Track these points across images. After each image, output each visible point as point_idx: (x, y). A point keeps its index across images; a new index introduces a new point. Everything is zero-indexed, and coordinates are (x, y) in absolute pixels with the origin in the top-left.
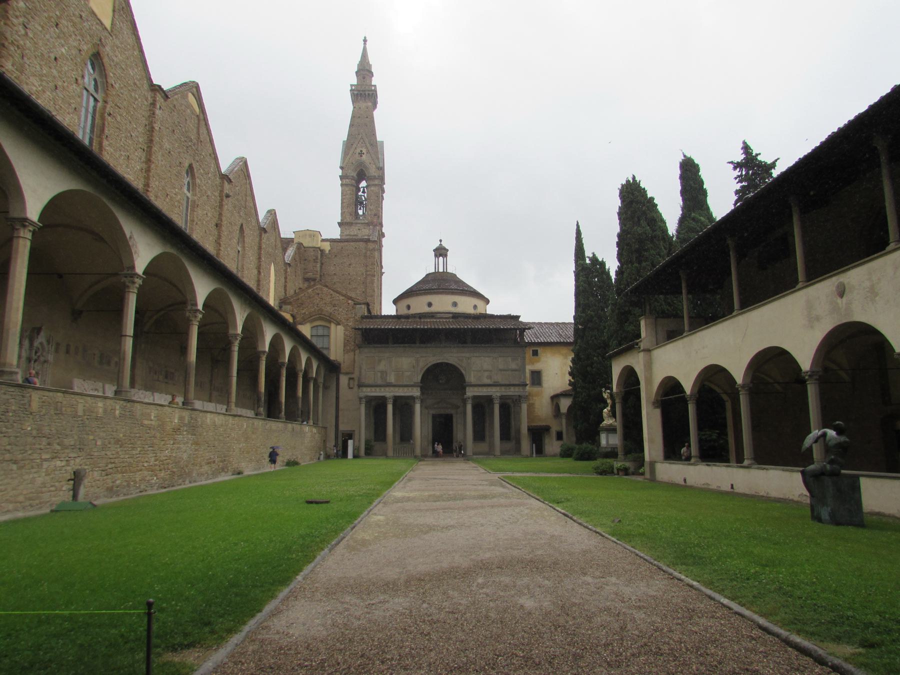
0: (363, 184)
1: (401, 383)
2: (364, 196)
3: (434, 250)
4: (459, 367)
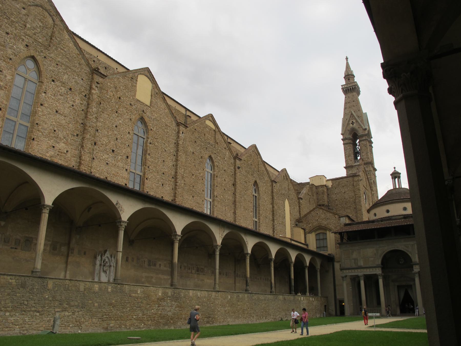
1: (368, 266)
2: (358, 148)
3: (391, 175)
4: (406, 251)
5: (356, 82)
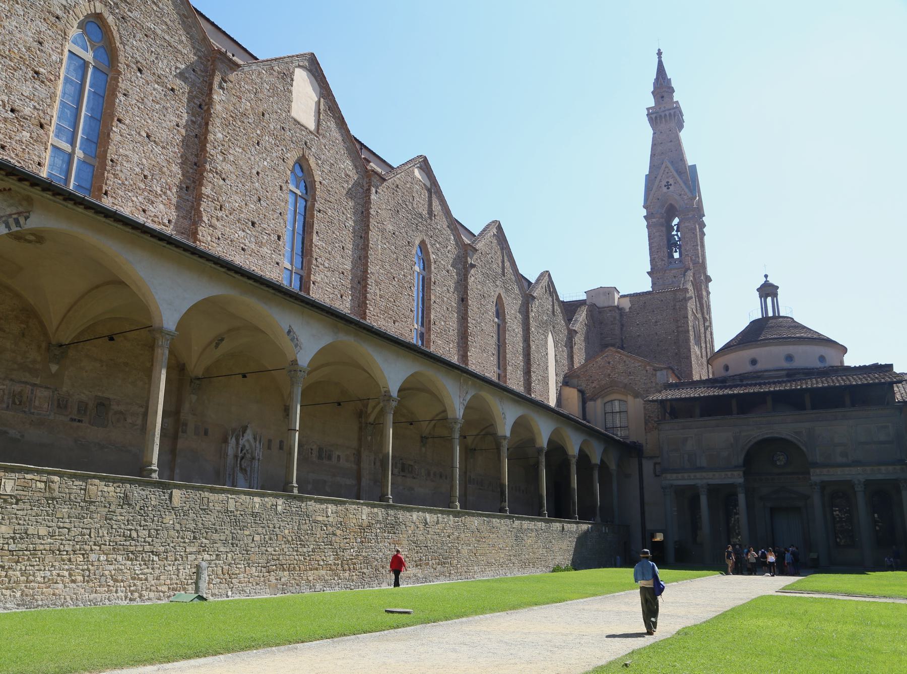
0: (676, 221)
2: (677, 235)
5: (677, 102)
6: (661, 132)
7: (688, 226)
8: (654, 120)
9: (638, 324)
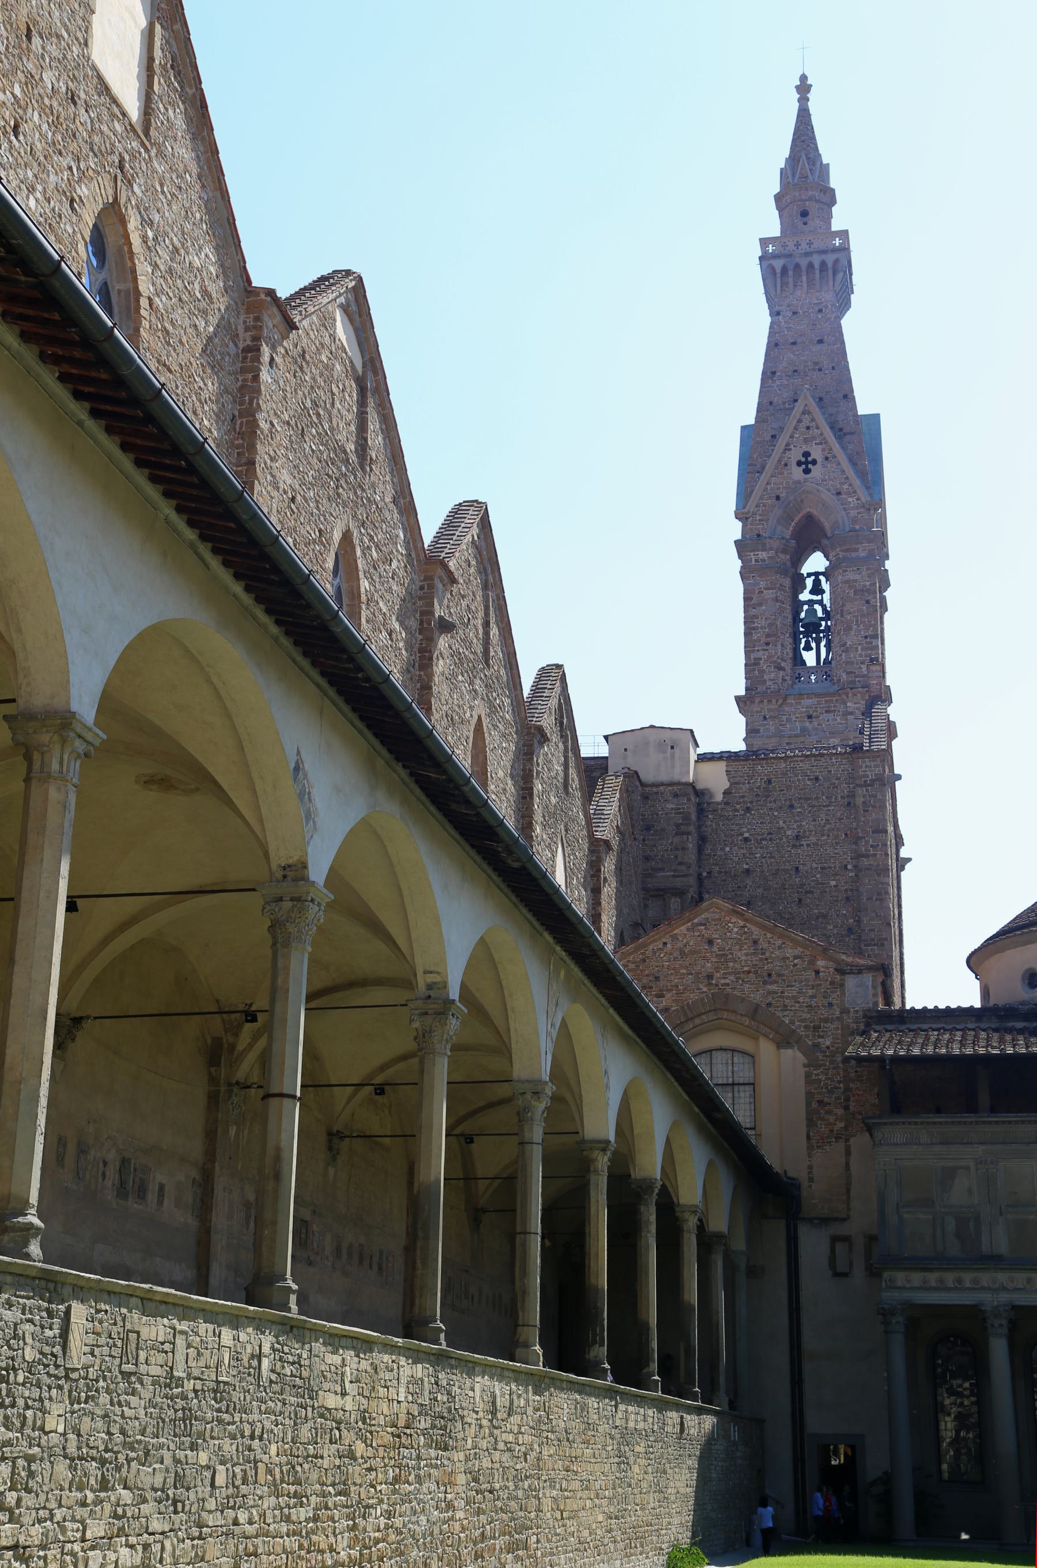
0: (816, 562)
2: (820, 602)
5: (844, 234)
6: (795, 313)
7: (856, 581)
8: (779, 275)
9: (746, 840)
